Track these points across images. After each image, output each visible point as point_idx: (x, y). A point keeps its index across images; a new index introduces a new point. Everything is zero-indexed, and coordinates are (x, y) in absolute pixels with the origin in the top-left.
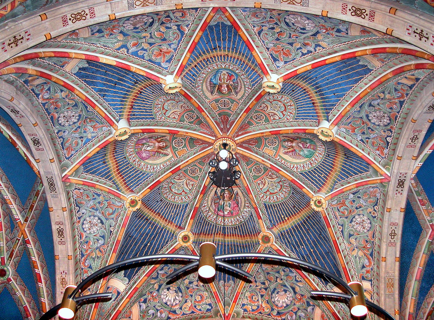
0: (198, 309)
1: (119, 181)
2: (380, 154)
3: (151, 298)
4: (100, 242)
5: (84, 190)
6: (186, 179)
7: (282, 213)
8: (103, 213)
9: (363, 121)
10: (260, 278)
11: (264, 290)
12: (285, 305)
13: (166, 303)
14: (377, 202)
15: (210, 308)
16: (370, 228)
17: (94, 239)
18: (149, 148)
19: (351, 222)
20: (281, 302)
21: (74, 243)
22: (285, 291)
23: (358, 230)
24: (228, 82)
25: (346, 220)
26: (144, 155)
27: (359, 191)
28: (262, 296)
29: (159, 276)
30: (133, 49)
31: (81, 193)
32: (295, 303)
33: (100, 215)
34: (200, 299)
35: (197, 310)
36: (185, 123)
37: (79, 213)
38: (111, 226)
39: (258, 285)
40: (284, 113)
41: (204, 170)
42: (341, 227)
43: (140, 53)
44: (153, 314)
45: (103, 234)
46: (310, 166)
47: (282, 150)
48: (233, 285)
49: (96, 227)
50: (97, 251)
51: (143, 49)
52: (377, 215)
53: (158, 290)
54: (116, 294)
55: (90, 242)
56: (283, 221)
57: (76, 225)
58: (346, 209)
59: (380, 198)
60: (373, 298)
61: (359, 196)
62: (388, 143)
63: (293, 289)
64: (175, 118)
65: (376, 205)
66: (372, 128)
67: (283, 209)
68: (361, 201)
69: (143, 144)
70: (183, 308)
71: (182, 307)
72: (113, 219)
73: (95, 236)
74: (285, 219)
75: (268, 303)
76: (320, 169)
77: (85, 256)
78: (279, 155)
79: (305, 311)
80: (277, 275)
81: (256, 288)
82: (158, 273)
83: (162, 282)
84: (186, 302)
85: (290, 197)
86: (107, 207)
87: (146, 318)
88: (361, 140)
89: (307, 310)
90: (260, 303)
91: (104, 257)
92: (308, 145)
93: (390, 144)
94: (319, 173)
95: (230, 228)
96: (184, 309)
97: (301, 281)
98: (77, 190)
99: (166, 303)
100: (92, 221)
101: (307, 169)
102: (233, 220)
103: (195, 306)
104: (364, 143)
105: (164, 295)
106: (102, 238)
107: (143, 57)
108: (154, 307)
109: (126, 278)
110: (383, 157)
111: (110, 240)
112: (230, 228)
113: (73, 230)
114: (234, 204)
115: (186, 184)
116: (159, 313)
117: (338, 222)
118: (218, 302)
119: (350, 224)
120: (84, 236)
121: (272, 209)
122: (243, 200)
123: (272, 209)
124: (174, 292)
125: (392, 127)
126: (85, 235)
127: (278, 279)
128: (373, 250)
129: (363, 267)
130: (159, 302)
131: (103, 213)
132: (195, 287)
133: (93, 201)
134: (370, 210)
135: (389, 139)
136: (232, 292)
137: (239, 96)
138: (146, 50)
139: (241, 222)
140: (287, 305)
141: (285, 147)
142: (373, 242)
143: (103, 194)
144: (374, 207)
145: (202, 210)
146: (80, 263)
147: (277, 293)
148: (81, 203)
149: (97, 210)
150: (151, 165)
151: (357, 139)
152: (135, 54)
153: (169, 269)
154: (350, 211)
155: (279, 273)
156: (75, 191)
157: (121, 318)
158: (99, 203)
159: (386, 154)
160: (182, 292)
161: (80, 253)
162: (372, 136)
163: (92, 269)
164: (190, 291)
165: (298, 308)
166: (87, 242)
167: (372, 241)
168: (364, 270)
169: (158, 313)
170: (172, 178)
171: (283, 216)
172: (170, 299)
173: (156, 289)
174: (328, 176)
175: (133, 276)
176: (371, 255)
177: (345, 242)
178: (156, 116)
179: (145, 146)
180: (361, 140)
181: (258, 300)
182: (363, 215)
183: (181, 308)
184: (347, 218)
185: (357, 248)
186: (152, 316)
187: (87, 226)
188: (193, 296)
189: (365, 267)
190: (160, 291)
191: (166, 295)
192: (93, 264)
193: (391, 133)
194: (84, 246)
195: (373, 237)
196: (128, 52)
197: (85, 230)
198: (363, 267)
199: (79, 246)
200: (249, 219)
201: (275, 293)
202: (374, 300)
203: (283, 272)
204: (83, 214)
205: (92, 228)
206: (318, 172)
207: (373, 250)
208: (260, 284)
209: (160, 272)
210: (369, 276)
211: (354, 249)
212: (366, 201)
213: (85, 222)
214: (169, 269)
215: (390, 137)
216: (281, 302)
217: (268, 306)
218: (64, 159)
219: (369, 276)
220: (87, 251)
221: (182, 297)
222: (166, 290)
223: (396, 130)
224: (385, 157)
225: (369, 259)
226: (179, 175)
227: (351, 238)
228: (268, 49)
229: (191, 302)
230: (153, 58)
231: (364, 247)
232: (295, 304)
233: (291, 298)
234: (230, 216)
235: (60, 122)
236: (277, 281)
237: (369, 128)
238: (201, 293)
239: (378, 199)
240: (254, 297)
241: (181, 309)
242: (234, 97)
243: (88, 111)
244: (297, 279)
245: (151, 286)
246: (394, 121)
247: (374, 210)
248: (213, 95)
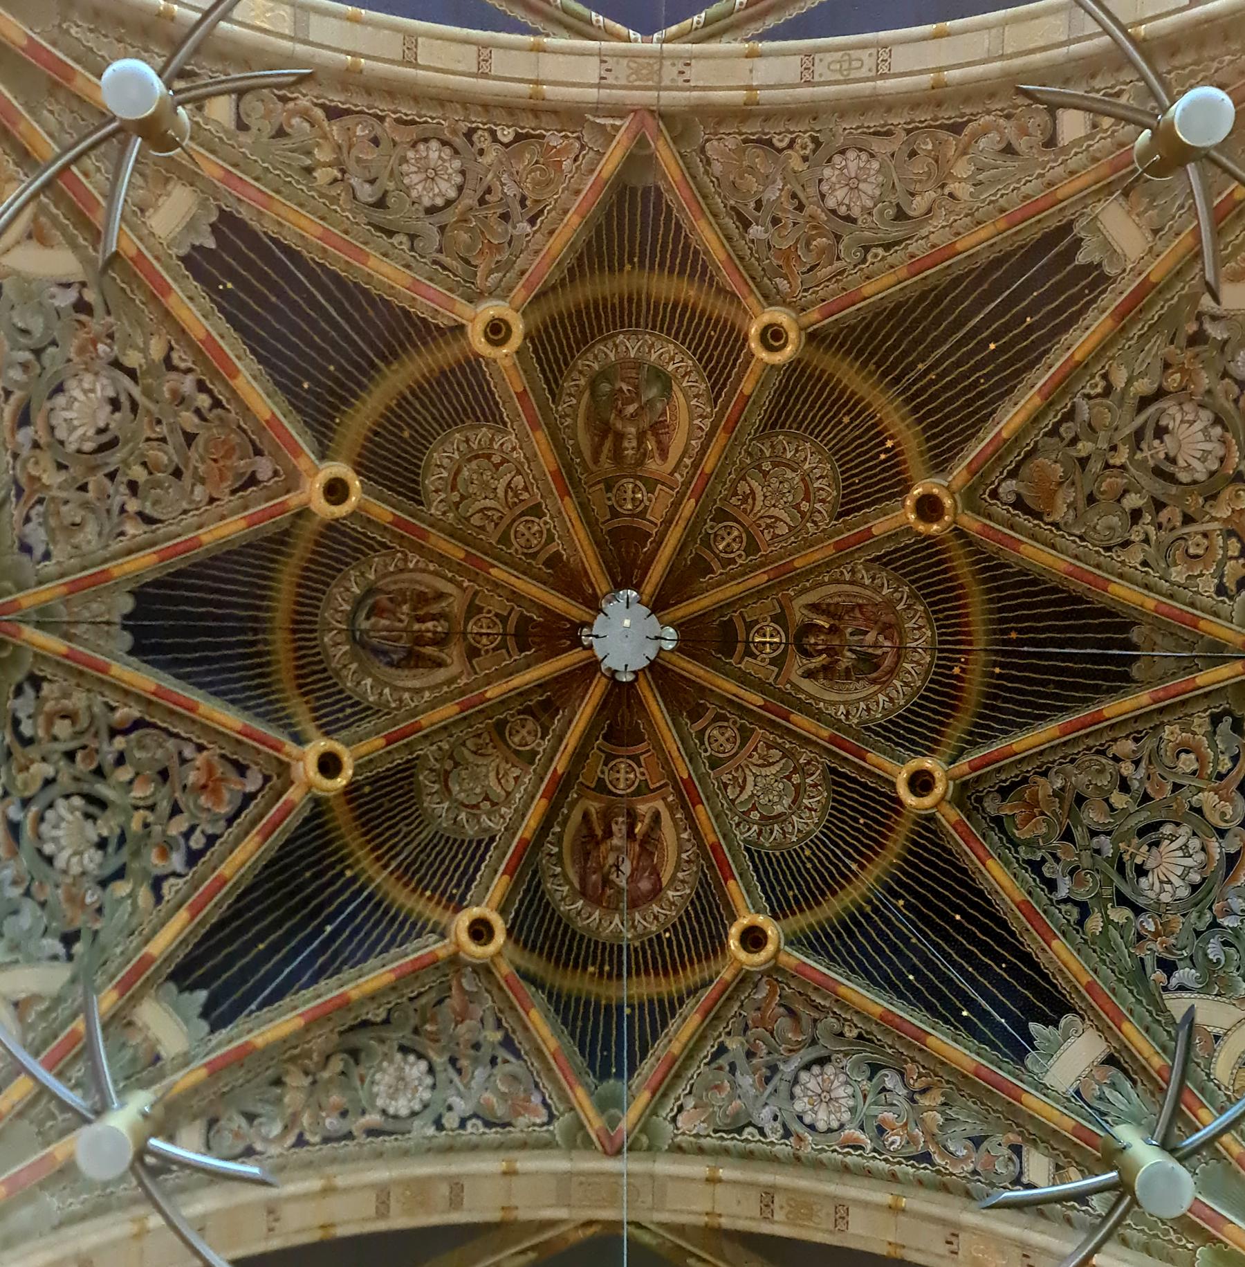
0: (1230, 765)
1: (691, 976)
2: (573, 156)
3: (1161, 943)
4: (889, 1085)
5: (690, 1093)
6: (747, 766)
7: (872, 458)
8: (790, 1051)
9: (456, 222)
10: (1110, 528)
11: (1165, 511)
12: (1218, 431)
13: (1194, 888)
14: (759, 141)
15: (1228, 720)
16: (861, 150)
17: (875, 1103)
18: (626, 868)
19: (854, 221)
20: (1208, 446)
21: (869, 1173)
22: (1160, 432)
23: (878, 192)
24: (403, 617)
25: (846, 239)
26: (645, 885)
27: (733, 208)
28: (1188, 520)
29: (1078, 898)
30: (177, 861)
31: (695, 1107)
32: (1202, 390)
33: (796, 1062)
34: (1192, 756)
35: (1236, 769)
36: (541, 750)
37: (767, 1130)
38: (841, 1034)
39: (1142, 537)
40: (496, 459)
41: (721, 708)
42: (874, 250)
43: (197, 842)
44: (1226, 943)
45: (865, 1067)
46: (694, 377)
47: (654, 466)
48: (1145, 629)
49: (836, 1084)
50: (924, 1101)
51: (187, 835)
52: (805, 132)
53: (1138, 910)
54: (1113, 1071)
55: (884, 1120)
56: (896, 455)
57: (807, 1151)
58: (808, 244)
59: (741, 134)
60: (1111, 88)
61: (752, 205)
62: (518, 137)
63: (1144, 402)
64: (516, 778)
65: (769, 143)
66: (480, 193)
67: (859, 455)
68: (772, 194)
69: (606, 882)
70: (1223, 825)
71: (1216, 829)
72: (815, 1021)
73: (865, 1097)
74: (893, 447)
75: (1214, 497)
76: (699, 345)
77: (932, 1149)
78: (672, 474)
79: (1228, 349)
80: (1095, 466)
81: (1153, 543)
82: (1066, 901)
83: (1108, 892)
84: (1199, 811)
85: (811, 434)
86: (772, 1034)
87: (1236, 974)
88: (532, 221)
89: (1225, 342)
90: (1215, 525)
91: (948, 1082)
92: (625, 387)
93: (523, 128)
94: (708, 345)
95: (941, 635)
96: (1226, 821)
97: (1105, 376)
98: (680, 1118)
99: (1194, 888)
100: (810, 1093)
101: (703, 386)
102: (911, 625)
103: (1220, 777)
104: (542, 211)
105: (1162, 891)
106: (879, 1074)
107: (211, 839)
108: (1198, 934)
109: (1063, 1022)
110: (577, 145)
111: (891, 1047)
112: (941, 635)
113: (818, 1165)
114: (855, 618)
115: (763, 766)
116: (1226, 922)
117: (855, 266)
118: (1191, 686)
119: (860, 222)
120: (858, 1134)
121: (857, 491)
122: (833, 588)
123: (857, 491)
124: (1154, 850)
125: (454, 132)
126: (852, 1132)
127: (1111, 462)
128: (935, 127)
129: (1009, 150)
130: (1184, 915)
131: (790, 1051)
132: (1142, 772)
133: (738, 1073)
134: (796, 163)
135: (506, 135)
136: (1172, 634)
137: (449, 588)
138: (192, 829)
139: (917, 597)
140: (1218, 421)
141: (643, 455)
142: (908, 132)
143: (720, 1035)
144: (780, 151)
145: (857, 724)
146: (951, 1174)
147: (1173, 461)
148: (736, 1115)
149: (774, 1069)
150: (678, 868)
151: (527, 235)
152: (193, 857)
153: (1058, 860)
154: (815, 227)
155: (1088, 458)
156: (679, 1125)
157: (1208, 1075)
158: (750, 1055)
159: (566, 137)
160: (1161, 824)
161: (913, 1166)
162: (511, 190)
163: (986, 1137)
164: (1157, 792)
165: (1222, 378)
166: (881, 1130)
167: (904, 134)
168: (1022, 144)
169: (1226, 924)
170: (730, 810)
171: (883, 457)
172: (1179, 871)
173: (1132, 916)
174: (709, 319)
175: (1060, 993)
176: (956, 129)
177: (924, 232)
178: (489, 829)
179: (613, 877)
180: (532, 221)
181: (1205, 535)
182: (820, 181)
184: (838, 238)
185: (943, 186)
186: (1232, 950)
187: (822, 1119)
188: (1178, 781)
189: (1009, 144)
190: (1141, 902)
191: (1161, 882)
192: (967, 1127)
193: (480, 132)
194: (893, 1143)
195: (889, 133)
196: (179, 876)
197: (835, 1125)
198: (1009, 150)
199: (886, 1160)
200: (895, 569)
201: (1172, 469)
202: (1118, 83)
203: (1080, 445)
204: (775, 1118)
205: (836, 1099)
206: (705, 350)
207: (935, 127)
208: (1135, 528)
209: (1063, 892)
210: (1038, 120)
211: (951, 195)
212: (767, 180)
213: (807, 1120)
214: (1058, 860)
215: (493, 133)
216: (1208, 446)
217: (1226, 494)
218: (547, 1131)
219: (1038, 120)
220: (912, 1140)
221: (1178, 824)
222: (1143, 880)
223: (455, 120)
224: (578, 138)
225: (975, 137)
226: (726, 786)
227: (911, 213)
228: (212, 500)
229: (1200, 790)
230: (225, 810)
231: (937, 162)
232: (1209, 392)
233: (1186, 407)
234: (900, 633)
235: (404, 1112)
236: (1123, 467)
237: (482, 201)
238: (1167, 751)
239: (745, 141)
240: (1192, 551)
241: (1226, 831)
242: (456, 605)
243: (386, 1022)
244: (1099, 390)
245: (1114, 933)
246: (425, 129)
247: (791, 145)
248: (449, 661)
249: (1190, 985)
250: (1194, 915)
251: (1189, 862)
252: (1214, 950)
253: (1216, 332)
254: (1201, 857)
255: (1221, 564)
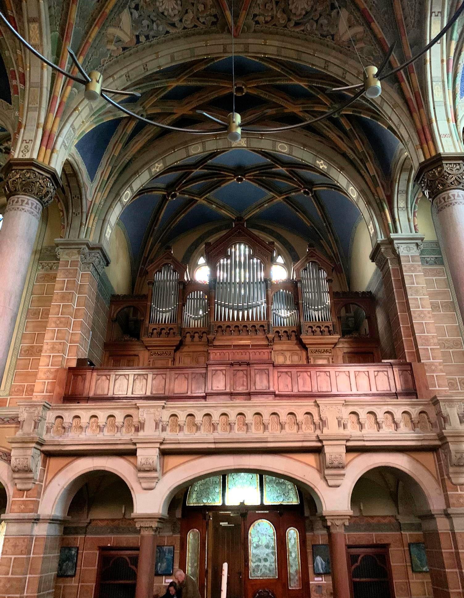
12: (304, 13)
13: (163, 13)
15: (215, 20)
34: (203, 9)
44: (148, 26)
70: (183, 21)
89: (330, 15)
90: (275, 13)
99: (163, 13)
103: (198, 19)
108: (149, 16)
140: (307, 13)
181: (272, 9)
183: (181, 21)
217: (285, 16)
249: (133, 15)
250: (154, 14)
251: (170, 10)
252: (145, 22)
253: (334, 13)
254: (172, 15)
255: (263, 15)
